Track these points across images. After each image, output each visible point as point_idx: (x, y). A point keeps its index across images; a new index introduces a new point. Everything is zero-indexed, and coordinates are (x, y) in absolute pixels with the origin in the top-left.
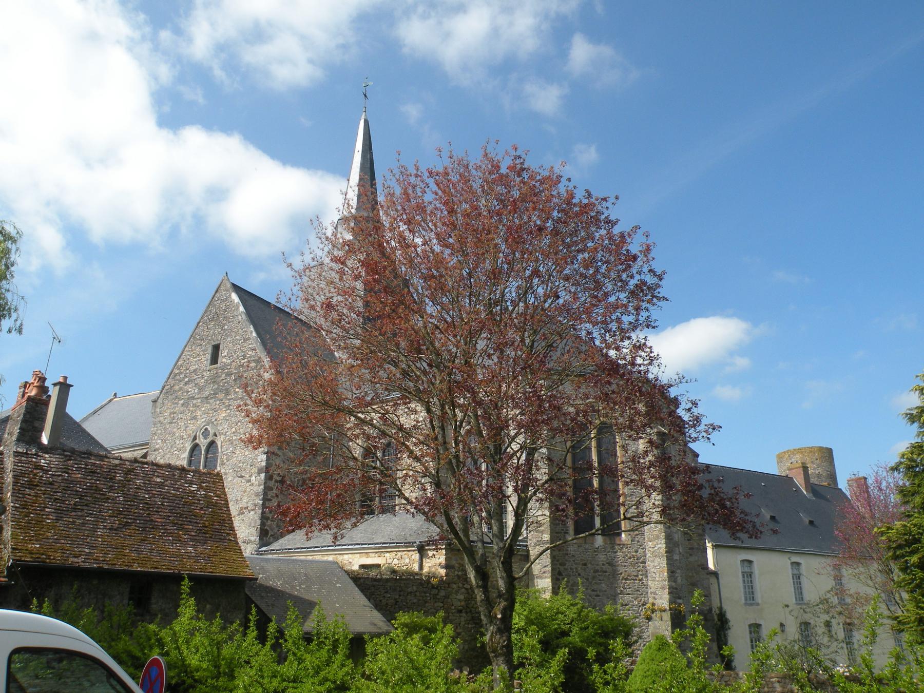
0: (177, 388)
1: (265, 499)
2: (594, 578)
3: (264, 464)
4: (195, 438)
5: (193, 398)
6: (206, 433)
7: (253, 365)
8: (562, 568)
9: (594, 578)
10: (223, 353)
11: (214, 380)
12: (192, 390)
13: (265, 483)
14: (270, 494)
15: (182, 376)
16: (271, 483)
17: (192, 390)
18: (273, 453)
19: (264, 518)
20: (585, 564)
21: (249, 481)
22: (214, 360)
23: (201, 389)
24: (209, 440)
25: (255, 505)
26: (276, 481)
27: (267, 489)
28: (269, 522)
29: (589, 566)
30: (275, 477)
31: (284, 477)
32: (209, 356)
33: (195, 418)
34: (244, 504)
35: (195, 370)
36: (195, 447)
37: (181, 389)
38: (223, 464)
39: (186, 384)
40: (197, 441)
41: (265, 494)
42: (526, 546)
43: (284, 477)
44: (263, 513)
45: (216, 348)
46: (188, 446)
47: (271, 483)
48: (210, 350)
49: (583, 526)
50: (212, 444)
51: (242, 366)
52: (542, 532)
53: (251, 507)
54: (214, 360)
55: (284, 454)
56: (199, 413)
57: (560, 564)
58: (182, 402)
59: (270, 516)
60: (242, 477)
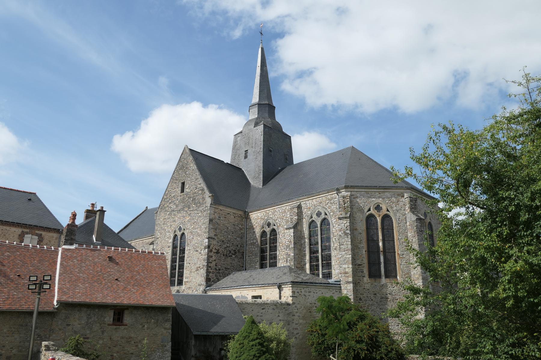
0: (166, 206)
1: (208, 262)
2: (381, 301)
3: (207, 244)
4: (175, 232)
5: (173, 211)
6: (180, 229)
7: (200, 192)
8: (361, 296)
9: (381, 301)
10: (187, 186)
11: (183, 201)
12: (173, 207)
13: (208, 254)
14: (211, 259)
17: (173, 207)
18: (212, 238)
19: (208, 272)
20: (375, 294)
21: (200, 253)
22: (182, 191)
23: (177, 206)
24: (181, 232)
25: (204, 266)
26: (214, 253)
27: (209, 257)
28: (211, 274)
29: (378, 295)
30: (214, 250)
31: (218, 250)
32: (180, 189)
33: (174, 221)
34: (198, 266)
35: (174, 196)
37: (168, 206)
38: (188, 245)
42: (340, 284)
43: (218, 250)
44: (207, 269)
45: (183, 184)
46: (172, 236)
48: (180, 185)
49: (374, 274)
50: (183, 234)
51: (195, 193)
52: (348, 277)
53: (201, 266)
54: (182, 191)
55: (218, 238)
56: (177, 219)
57: (361, 294)
59: (211, 271)
60: (197, 251)
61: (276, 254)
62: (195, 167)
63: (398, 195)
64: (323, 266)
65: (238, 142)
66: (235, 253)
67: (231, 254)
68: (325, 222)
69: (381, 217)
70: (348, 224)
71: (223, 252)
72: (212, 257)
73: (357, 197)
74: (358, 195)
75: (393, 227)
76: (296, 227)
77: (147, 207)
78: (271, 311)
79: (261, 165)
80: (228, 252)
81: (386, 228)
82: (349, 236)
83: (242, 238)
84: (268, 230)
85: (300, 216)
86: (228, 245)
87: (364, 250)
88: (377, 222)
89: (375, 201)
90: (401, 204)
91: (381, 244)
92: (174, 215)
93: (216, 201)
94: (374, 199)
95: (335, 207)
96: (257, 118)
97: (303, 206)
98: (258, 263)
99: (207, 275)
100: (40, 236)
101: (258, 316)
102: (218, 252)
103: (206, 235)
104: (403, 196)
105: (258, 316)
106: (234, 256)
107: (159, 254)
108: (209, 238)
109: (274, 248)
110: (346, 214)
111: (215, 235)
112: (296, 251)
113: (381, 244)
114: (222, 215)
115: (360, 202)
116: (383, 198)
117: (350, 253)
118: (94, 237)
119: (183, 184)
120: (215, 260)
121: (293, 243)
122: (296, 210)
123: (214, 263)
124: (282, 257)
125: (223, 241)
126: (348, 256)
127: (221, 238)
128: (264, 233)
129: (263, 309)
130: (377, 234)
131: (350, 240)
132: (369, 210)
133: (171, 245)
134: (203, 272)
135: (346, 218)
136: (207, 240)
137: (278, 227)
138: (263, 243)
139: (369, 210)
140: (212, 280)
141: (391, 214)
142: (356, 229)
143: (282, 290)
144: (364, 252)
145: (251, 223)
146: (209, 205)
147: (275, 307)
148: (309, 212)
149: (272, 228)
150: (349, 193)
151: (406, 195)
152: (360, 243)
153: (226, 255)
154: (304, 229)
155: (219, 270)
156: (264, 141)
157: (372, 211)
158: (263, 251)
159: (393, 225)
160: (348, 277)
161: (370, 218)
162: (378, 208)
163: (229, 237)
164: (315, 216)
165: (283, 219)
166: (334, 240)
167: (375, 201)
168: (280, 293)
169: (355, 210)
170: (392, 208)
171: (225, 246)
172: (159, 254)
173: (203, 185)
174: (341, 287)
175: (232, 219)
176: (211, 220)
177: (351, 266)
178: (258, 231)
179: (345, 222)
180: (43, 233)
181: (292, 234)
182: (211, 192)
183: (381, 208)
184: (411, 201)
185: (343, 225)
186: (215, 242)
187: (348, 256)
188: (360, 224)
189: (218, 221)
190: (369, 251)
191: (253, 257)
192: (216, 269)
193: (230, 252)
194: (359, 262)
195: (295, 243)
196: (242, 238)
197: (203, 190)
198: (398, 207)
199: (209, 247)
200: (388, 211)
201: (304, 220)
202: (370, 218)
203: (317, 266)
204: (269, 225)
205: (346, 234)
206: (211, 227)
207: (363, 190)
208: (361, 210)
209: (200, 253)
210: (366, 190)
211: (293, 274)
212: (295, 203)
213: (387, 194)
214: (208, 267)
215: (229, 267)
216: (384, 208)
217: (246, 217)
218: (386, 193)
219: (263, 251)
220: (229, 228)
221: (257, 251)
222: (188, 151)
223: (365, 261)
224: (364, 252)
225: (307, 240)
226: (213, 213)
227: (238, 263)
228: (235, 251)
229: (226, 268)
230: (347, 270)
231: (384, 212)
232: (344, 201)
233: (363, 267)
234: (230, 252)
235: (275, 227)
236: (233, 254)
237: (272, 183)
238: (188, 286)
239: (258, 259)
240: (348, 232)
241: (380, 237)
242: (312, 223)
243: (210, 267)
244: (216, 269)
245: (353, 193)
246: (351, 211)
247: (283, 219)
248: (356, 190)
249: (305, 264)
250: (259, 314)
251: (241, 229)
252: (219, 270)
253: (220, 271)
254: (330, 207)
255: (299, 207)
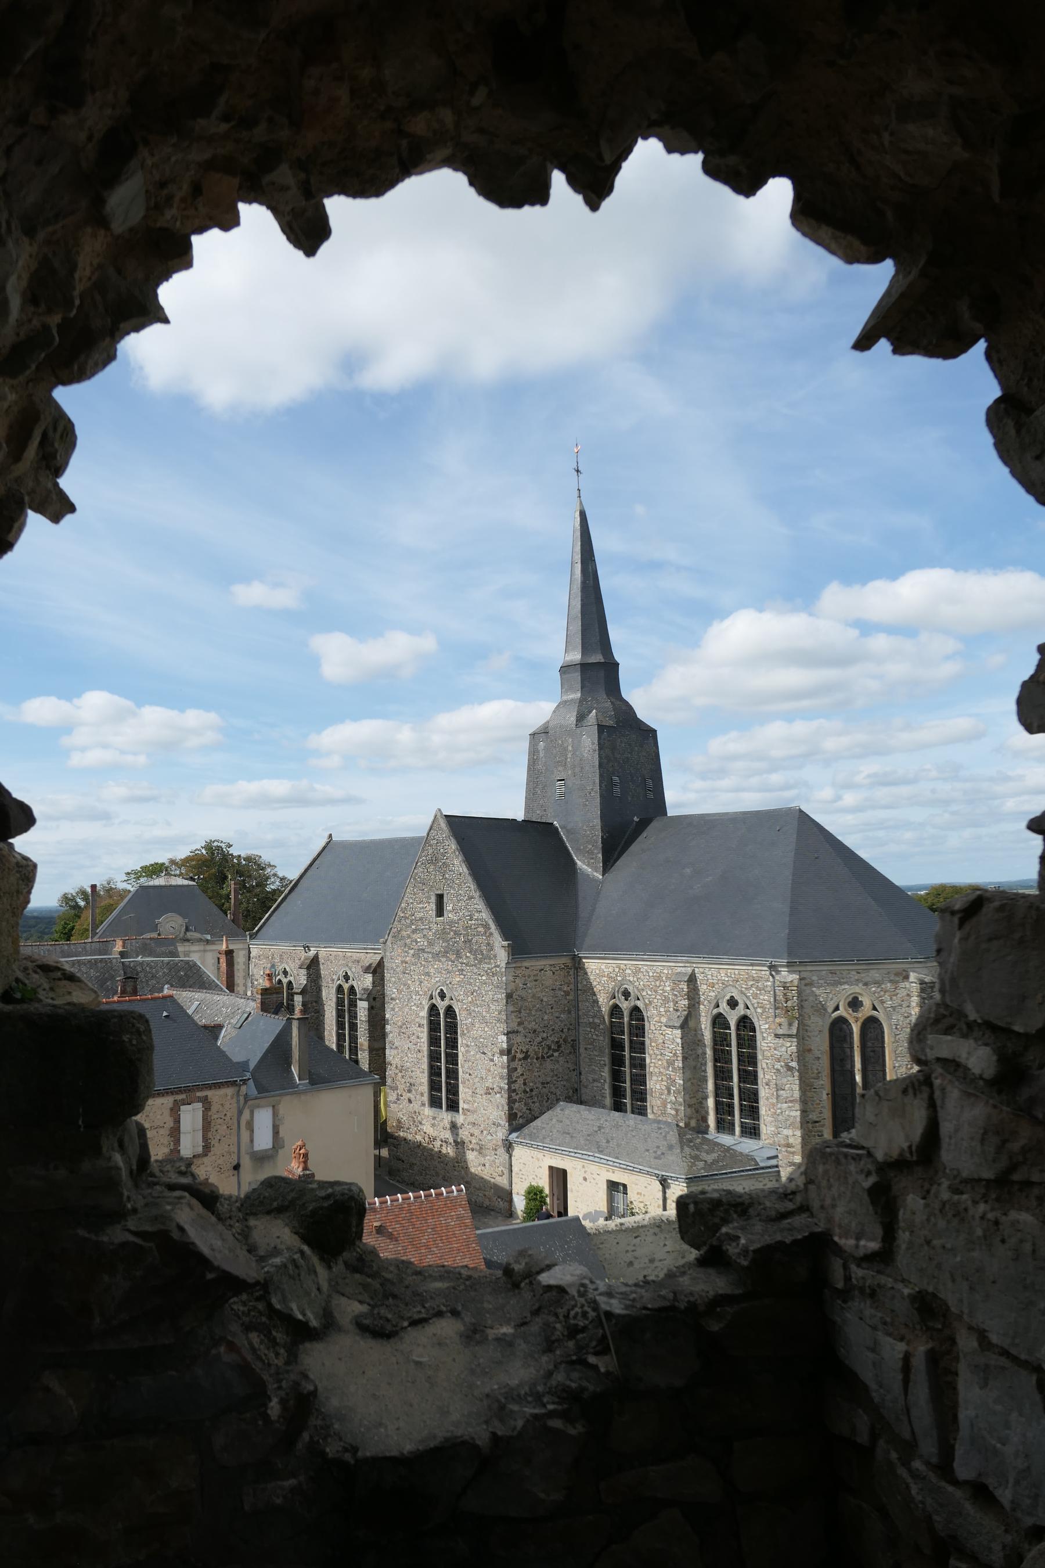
0: (404, 933)
1: (510, 1083)
3: (505, 1046)
4: (431, 998)
10: (448, 907)
12: (423, 943)
13: (508, 1066)
15: (408, 921)
16: (514, 1065)
18: (513, 1032)
19: (511, 1102)
21: (492, 1060)
22: (440, 911)
23: (431, 944)
25: (501, 1088)
26: (520, 1060)
27: (511, 1070)
28: (517, 1104)
33: (428, 974)
34: (489, 1084)
35: (421, 919)
36: (433, 1009)
37: (409, 937)
38: (463, 1034)
39: (414, 931)
40: (434, 1001)
41: (510, 1076)
42: (777, 1166)
44: (510, 1097)
45: (440, 898)
47: (514, 1065)
48: (433, 899)
52: (793, 1153)
53: (496, 1089)
54: (440, 911)
55: (524, 1028)
56: (432, 970)
58: (412, 952)
59: (517, 1098)
60: (484, 1053)
61: (644, 1059)
62: (464, 869)
63: (897, 974)
64: (741, 1111)
65: (542, 755)
66: (559, 1046)
67: (551, 1052)
68: (745, 1023)
69: (859, 1024)
70: (794, 1048)
71: (536, 1053)
72: (516, 1069)
73: (811, 984)
74: (815, 978)
75: (883, 1042)
76: (688, 1024)
77: (330, 836)
78: (650, 1239)
79: (597, 822)
80: (546, 1050)
81: (869, 1044)
82: (796, 1074)
83: (569, 1012)
84: (625, 1006)
85: (693, 999)
86: (545, 1035)
87: (825, 1093)
88: (851, 1033)
89: (848, 990)
90: (902, 993)
91: (858, 1078)
92: (426, 960)
93: (518, 950)
94: (847, 987)
95: (766, 998)
96: (581, 701)
97: (700, 977)
98: (607, 1069)
99: (510, 1108)
100: (206, 1102)
101: (627, 1251)
102: (525, 1058)
103: (503, 1027)
104: (907, 977)
105: (627, 1251)
106: (556, 1054)
107: (455, 1193)
108: (507, 1034)
109: (639, 1047)
110: (790, 1025)
111: (519, 1024)
112: (688, 1074)
113: (858, 1078)
114: (529, 976)
115: (818, 992)
116: (866, 984)
117: (797, 1106)
118: (295, 1070)
119: (440, 898)
120: (522, 1075)
121: (680, 1058)
122: (684, 987)
123: (520, 1081)
124: (656, 1070)
125: (535, 1031)
126: (794, 1113)
127: (529, 1027)
128: (615, 1010)
129: (636, 1237)
130: (852, 1057)
131: (797, 1082)
132: (837, 1008)
133: (425, 1022)
134: (501, 1099)
135: (790, 1036)
136: (504, 1038)
137: (646, 1005)
138: (615, 1029)
139: (837, 1008)
140: (519, 1114)
141: (881, 1016)
142: (810, 1050)
143: (669, 1187)
144: (824, 1096)
145: (588, 980)
146: (503, 965)
147: (657, 1230)
148: (712, 994)
149: (632, 1004)
150: (795, 977)
151: (913, 977)
152: (818, 1078)
153: (543, 1057)
154: (703, 1026)
155: (531, 1090)
156: (600, 765)
157: (842, 1012)
158: (616, 1045)
159: (883, 1037)
160: (793, 1153)
161: (839, 1029)
162: (855, 1004)
163: (546, 1018)
164: (724, 1008)
165: (656, 992)
166: (764, 1066)
167: (848, 990)
168: (664, 1193)
169: (808, 1010)
170: (882, 1002)
171: (539, 1039)
172: (455, 1193)
173: (486, 915)
174: (779, 1172)
175: (548, 979)
176: (509, 996)
177: (798, 1133)
178: (604, 1003)
179: (789, 1044)
180: (209, 1093)
181: (679, 1041)
182: (506, 935)
183: (861, 1004)
184: (922, 990)
185: (784, 1049)
186: (519, 1039)
187: (794, 1113)
188: (818, 1039)
189: (523, 993)
190: (834, 1095)
191: (596, 1053)
192: (525, 1092)
193: (549, 1048)
194: (813, 1116)
195: (685, 1059)
196: (569, 1012)
197: (486, 927)
198: (897, 1001)
199: (509, 1052)
200: (875, 1008)
201: (702, 1006)
202: (839, 1029)
203: (731, 1106)
204: (626, 994)
205: (790, 1069)
206: (511, 1008)
207: (826, 968)
208: (821, 1009)
209: (492, 1060)
210: (830, 968)
211: (687, 1150)
212: (681, 966)
213: (875, 975)
214: (510, 1091)
215: (549, 1079)
216: (867, 1002)
217: (577, 966)
218: (872, 972)
219: (616, 1045)
220: (545, 999)
221: (604, 1042)
222: (443, 824)
223: (827, 1114)
224: (825, 1097)
225: (709, 1052)
226: (511, 978)
227: (566, 1065)
228: (557, 1042)
229: (543, 1083)
230: (791, 1140)
231: (866, 1011)
232: (785, 994)
233: (823, 1126)
234: (549, 1048)
235: (640, 1004)
236: (555, 1051)
237: (628, 864)
238: (471, 1118)
239: (606, 1059)
240: (794, 1064)
241: (858, 1065)
242: (719, 1021)
243: (514, 1091)
244: (525, 1092)
245: (804, 974)
246: (799, 1011)
247: (656, 992)
248: (809, 968)
249: (706, 1098)
250: (630, 1248)
251: (567, 993)
252: (531, 1090)
253: (534, 1093)
254: (755, 996)
255: (692, 979)
